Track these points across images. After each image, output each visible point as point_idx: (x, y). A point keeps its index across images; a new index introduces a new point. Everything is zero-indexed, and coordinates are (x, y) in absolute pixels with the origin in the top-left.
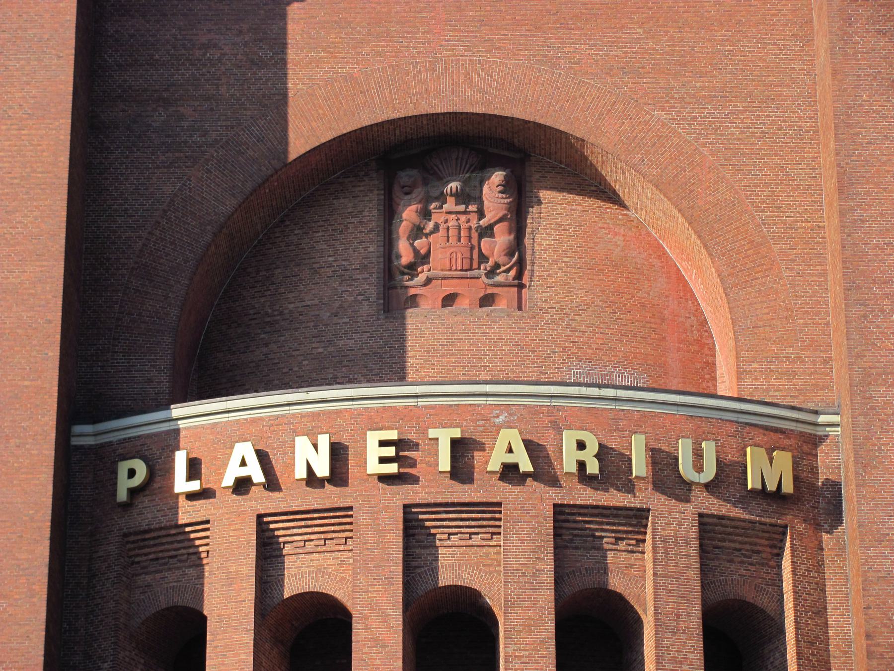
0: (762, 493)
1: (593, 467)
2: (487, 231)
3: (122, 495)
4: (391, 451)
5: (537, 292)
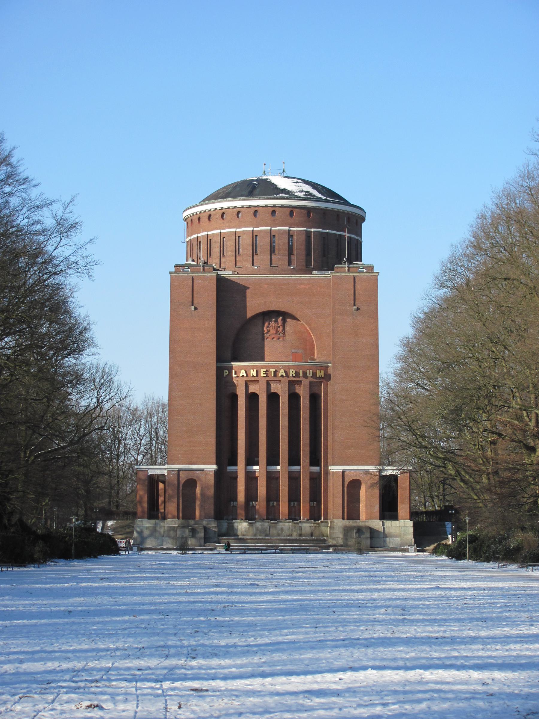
0: (319, 377)
1: (294, 375)
2: (279, 327)
3: (225, 376)
5: (287, 337)
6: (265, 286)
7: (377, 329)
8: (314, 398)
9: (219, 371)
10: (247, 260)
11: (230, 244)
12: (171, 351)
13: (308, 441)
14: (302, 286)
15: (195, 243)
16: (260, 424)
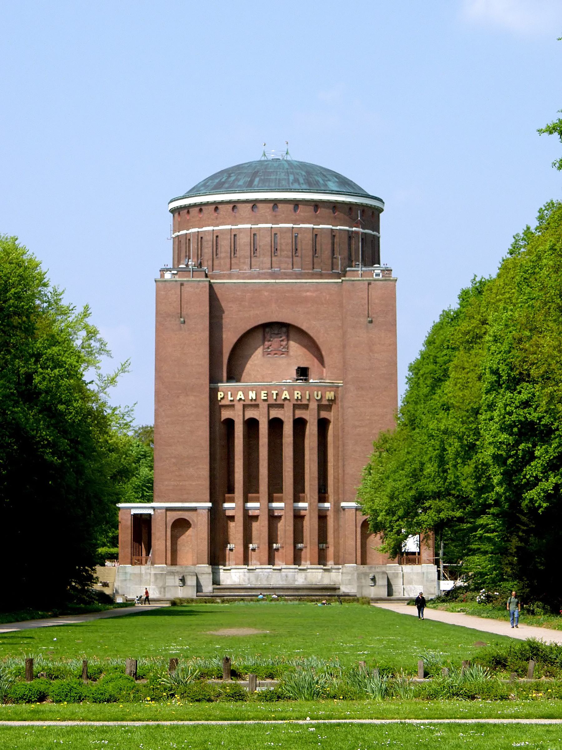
1: (300, 398)
2: (282, 341)
3: (219, 399)
4: (266, 395)
5: (291, 353)
6: (266, 294)
7: (395, 344)
8: (323, 424)
9: (213, 392)
10: (244, 263)
11: (225, 244)
12: (158, 370)
13: (316, 474)
14: (308, 294)
15: (183, 241)
16: (261, 454)
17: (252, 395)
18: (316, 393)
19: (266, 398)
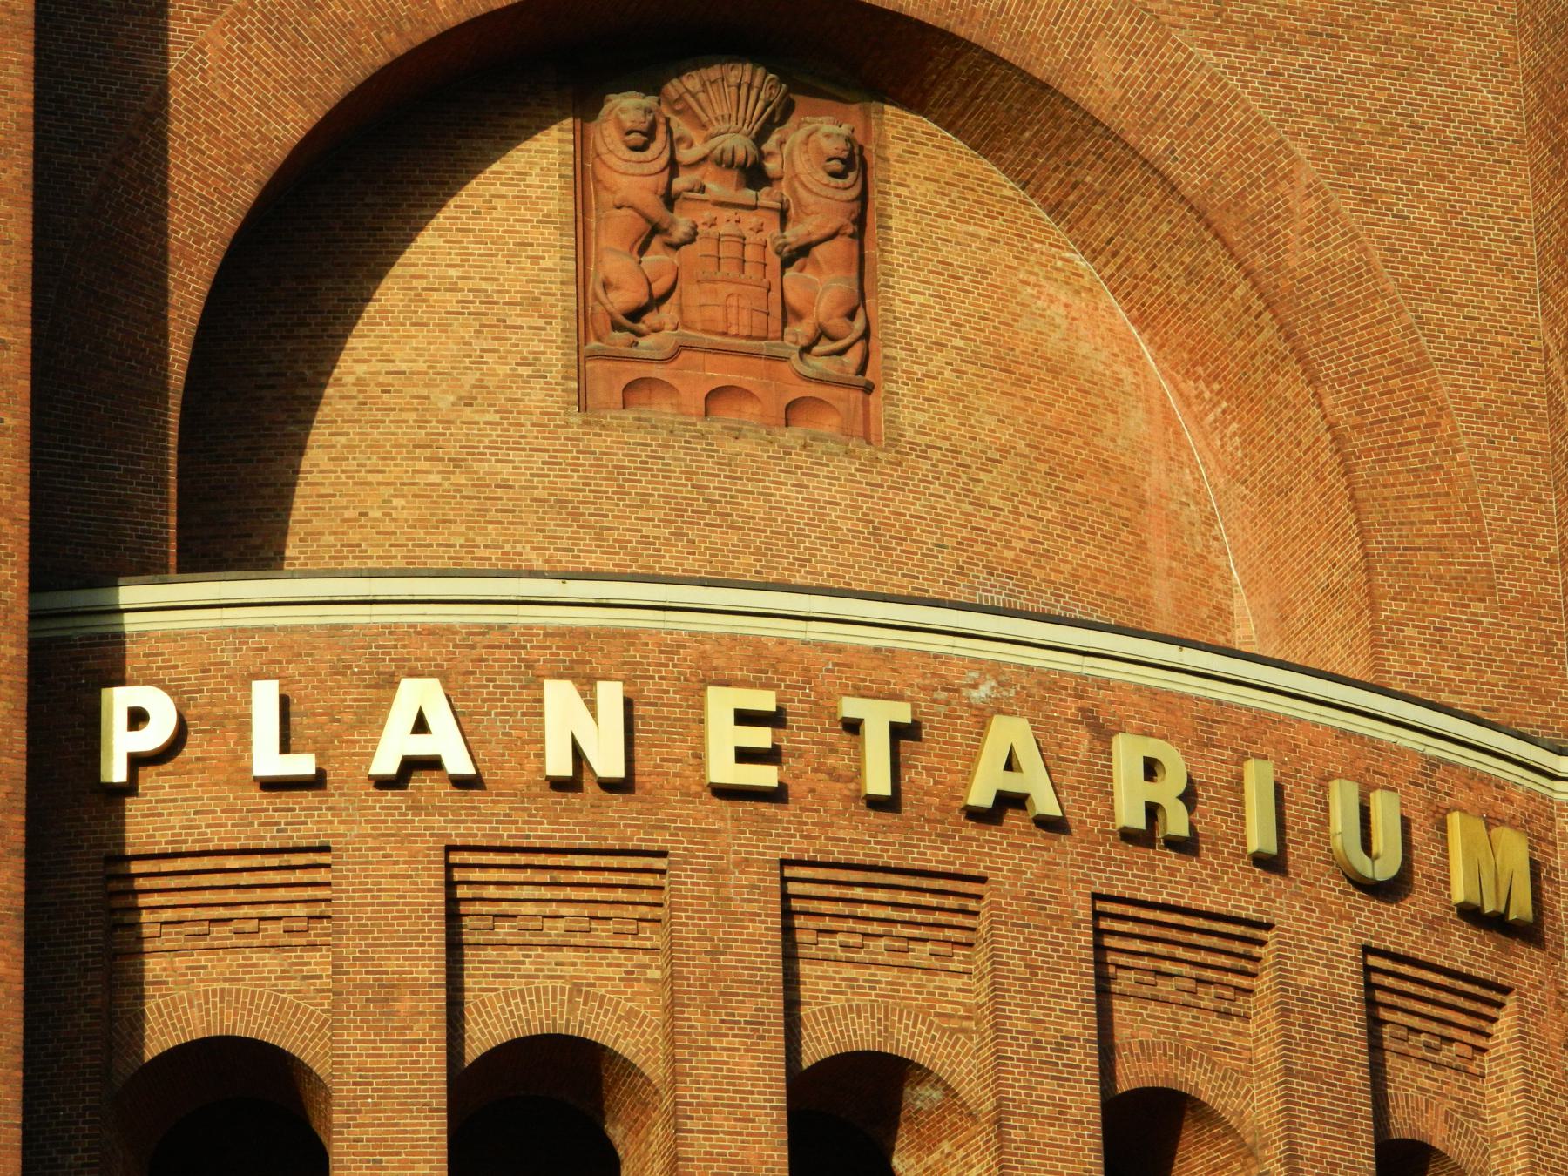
1: (1177, 822)
4: (760, 737)
5: (908, 410)
17: (581, 725)
18: (1342, 799)
19: (765, 775)
